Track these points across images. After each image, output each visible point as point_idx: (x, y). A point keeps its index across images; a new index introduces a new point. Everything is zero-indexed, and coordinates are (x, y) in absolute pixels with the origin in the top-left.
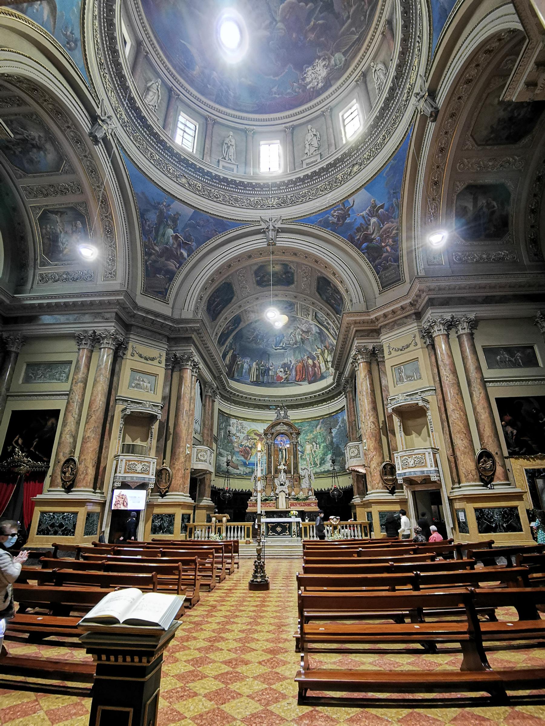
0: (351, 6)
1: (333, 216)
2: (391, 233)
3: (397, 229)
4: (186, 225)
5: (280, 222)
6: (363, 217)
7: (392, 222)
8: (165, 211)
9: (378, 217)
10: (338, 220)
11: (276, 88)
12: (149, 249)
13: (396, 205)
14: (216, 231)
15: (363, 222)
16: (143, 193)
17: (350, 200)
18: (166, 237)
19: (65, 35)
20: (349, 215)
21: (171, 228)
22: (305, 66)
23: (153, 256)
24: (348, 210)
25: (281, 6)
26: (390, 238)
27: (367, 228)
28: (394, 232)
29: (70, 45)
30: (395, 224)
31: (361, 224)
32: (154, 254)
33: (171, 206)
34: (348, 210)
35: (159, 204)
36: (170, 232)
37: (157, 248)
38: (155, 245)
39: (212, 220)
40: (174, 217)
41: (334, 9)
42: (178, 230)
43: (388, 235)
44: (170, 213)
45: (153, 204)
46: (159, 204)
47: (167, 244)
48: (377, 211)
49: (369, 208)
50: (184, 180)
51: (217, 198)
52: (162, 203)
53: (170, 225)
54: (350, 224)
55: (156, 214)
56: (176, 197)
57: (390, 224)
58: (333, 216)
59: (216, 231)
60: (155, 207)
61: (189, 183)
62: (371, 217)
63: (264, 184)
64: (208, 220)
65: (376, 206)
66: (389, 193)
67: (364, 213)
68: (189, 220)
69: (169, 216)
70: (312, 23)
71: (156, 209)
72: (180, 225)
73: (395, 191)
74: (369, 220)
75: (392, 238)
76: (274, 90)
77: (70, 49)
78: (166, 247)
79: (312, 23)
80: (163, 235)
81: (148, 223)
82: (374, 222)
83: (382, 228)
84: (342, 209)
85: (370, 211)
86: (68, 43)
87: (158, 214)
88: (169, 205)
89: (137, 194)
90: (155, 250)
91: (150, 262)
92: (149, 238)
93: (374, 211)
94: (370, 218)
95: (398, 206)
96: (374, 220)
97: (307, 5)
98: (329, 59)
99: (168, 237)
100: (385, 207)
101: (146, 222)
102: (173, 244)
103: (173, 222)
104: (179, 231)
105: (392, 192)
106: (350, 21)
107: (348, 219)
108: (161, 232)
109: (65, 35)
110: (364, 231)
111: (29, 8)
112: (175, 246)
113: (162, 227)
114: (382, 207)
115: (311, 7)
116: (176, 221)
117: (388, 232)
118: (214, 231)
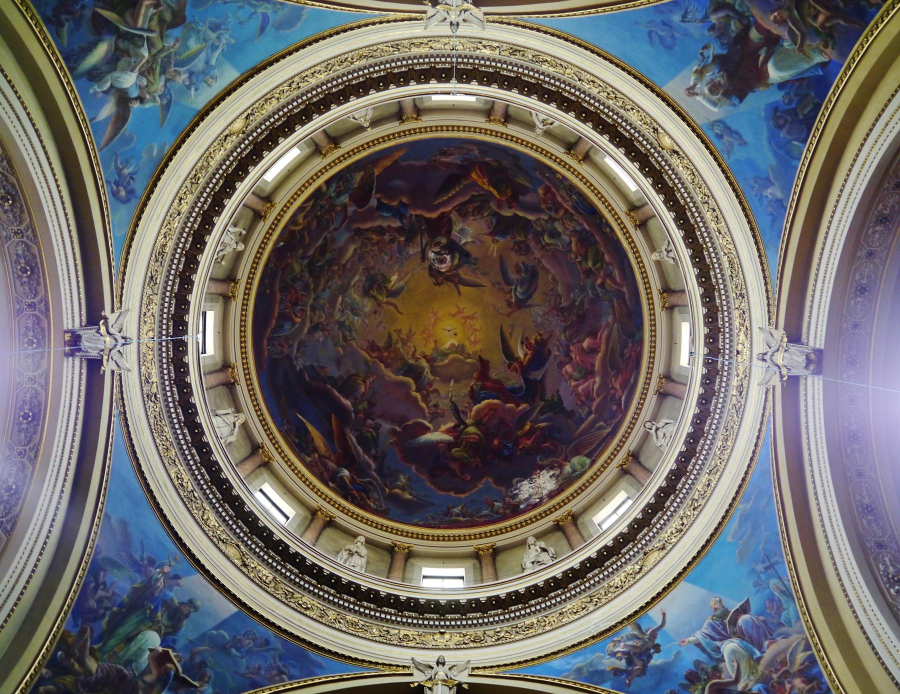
0: (593, 400)
1: (613, 654)
2: (792, 663)
3: (808, 647)
4: (203, 638)
5: (467, 672)
6: (698, 645)
7: (786, 636)
8: (161, 584)
9: (741, 635)
10: (630, 662)
11: (460, 508)
12: (69, 655)
13: (782, 592)
14: (281, 672)
15: (703, 657)
16: (124, 523)
17: (654, 613)
18: (134, 647)
19: (119, 172)
20: (657, 648)
21: (158, 631)
22: (515, 480)
23: (69, 679)
24: (654, 635)
25: (475, 408)
26: (794, 676)
27: (717, 671)
28: (801, 657)
29: (119, 191)
30: (795, 639)
31: (697, 663)
32: (76, 674)
33: (182, 582)
34: (654, 635)
35: (152, 562)
36: (152, 639)
37: (93, 665)
38: (92, 653)
39: (279, 645)
40: (177, 609)
41: (564, 408)
42: (174, 641)
43: (787, 672)
44: (171, 594)
45: (137, 557)
46: (152, 562)
47: (128, 663)
48: (734, 622)
49: (709, 620)
50: (231, 551)
51: (307, 609)
52: (161, 566)
53: (159, 622)
54: (664, 671)
55: (133, 581)
56: (202, 567)
57: (781, 643)
58: (613, 654)
59: (281, 672)
60: (137, 566)
61: (243, 561)
62: (721, 640)
63: (429, 602)
64: (267, 642)
65: (726, 612)
66: (753, 571)
67: (698, 636)
68: (217, 628)
69: (167, 603)
70: (527, 427)
71: (139, 571)
72: (187, 631)
73: (767, 564)
74: (718, 650)
75: (801, 673)
76: (457, 510)
77: (115, 194)
78: (119, 672)
79: (527, 427)
80: (129, 639)
81: (100, 593)
82: (734, 652)
83: (759, 659)
84: (634, 637)
85: (713, 628)
86: (117, 184)
87: (136, 585)
88: (177, 577)
89: (107, 516)
90: (82, 663)
91: (51, 687)
92: (83, 632)
93: (725, 624)
94: (718, 643)
95: (787, 593)
96: (729, 647)
97: (518, 406)
98: (561, 467)
99: (140, 651)
100: (754, 607)
101: (96, 588)
102: (147, 671)
103: (170, 618)
104: (177, 646)
105: (760, 567)
106: (593, 416)
107: (655, 656)
108: (124, 630)
109: (119, 172)
110: (710, 679)
111: (84, 79)
112: (148, 678)
113: (133, 620)
114: (744, 609)
115: (524, 409)
116: (180, 621)
117: (783, 663)
118: (275, 672)
